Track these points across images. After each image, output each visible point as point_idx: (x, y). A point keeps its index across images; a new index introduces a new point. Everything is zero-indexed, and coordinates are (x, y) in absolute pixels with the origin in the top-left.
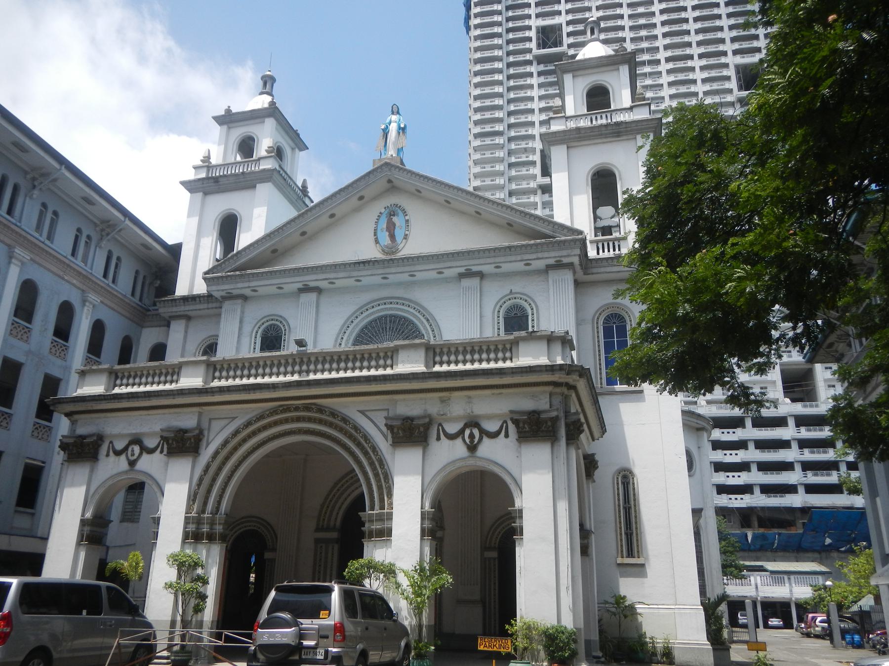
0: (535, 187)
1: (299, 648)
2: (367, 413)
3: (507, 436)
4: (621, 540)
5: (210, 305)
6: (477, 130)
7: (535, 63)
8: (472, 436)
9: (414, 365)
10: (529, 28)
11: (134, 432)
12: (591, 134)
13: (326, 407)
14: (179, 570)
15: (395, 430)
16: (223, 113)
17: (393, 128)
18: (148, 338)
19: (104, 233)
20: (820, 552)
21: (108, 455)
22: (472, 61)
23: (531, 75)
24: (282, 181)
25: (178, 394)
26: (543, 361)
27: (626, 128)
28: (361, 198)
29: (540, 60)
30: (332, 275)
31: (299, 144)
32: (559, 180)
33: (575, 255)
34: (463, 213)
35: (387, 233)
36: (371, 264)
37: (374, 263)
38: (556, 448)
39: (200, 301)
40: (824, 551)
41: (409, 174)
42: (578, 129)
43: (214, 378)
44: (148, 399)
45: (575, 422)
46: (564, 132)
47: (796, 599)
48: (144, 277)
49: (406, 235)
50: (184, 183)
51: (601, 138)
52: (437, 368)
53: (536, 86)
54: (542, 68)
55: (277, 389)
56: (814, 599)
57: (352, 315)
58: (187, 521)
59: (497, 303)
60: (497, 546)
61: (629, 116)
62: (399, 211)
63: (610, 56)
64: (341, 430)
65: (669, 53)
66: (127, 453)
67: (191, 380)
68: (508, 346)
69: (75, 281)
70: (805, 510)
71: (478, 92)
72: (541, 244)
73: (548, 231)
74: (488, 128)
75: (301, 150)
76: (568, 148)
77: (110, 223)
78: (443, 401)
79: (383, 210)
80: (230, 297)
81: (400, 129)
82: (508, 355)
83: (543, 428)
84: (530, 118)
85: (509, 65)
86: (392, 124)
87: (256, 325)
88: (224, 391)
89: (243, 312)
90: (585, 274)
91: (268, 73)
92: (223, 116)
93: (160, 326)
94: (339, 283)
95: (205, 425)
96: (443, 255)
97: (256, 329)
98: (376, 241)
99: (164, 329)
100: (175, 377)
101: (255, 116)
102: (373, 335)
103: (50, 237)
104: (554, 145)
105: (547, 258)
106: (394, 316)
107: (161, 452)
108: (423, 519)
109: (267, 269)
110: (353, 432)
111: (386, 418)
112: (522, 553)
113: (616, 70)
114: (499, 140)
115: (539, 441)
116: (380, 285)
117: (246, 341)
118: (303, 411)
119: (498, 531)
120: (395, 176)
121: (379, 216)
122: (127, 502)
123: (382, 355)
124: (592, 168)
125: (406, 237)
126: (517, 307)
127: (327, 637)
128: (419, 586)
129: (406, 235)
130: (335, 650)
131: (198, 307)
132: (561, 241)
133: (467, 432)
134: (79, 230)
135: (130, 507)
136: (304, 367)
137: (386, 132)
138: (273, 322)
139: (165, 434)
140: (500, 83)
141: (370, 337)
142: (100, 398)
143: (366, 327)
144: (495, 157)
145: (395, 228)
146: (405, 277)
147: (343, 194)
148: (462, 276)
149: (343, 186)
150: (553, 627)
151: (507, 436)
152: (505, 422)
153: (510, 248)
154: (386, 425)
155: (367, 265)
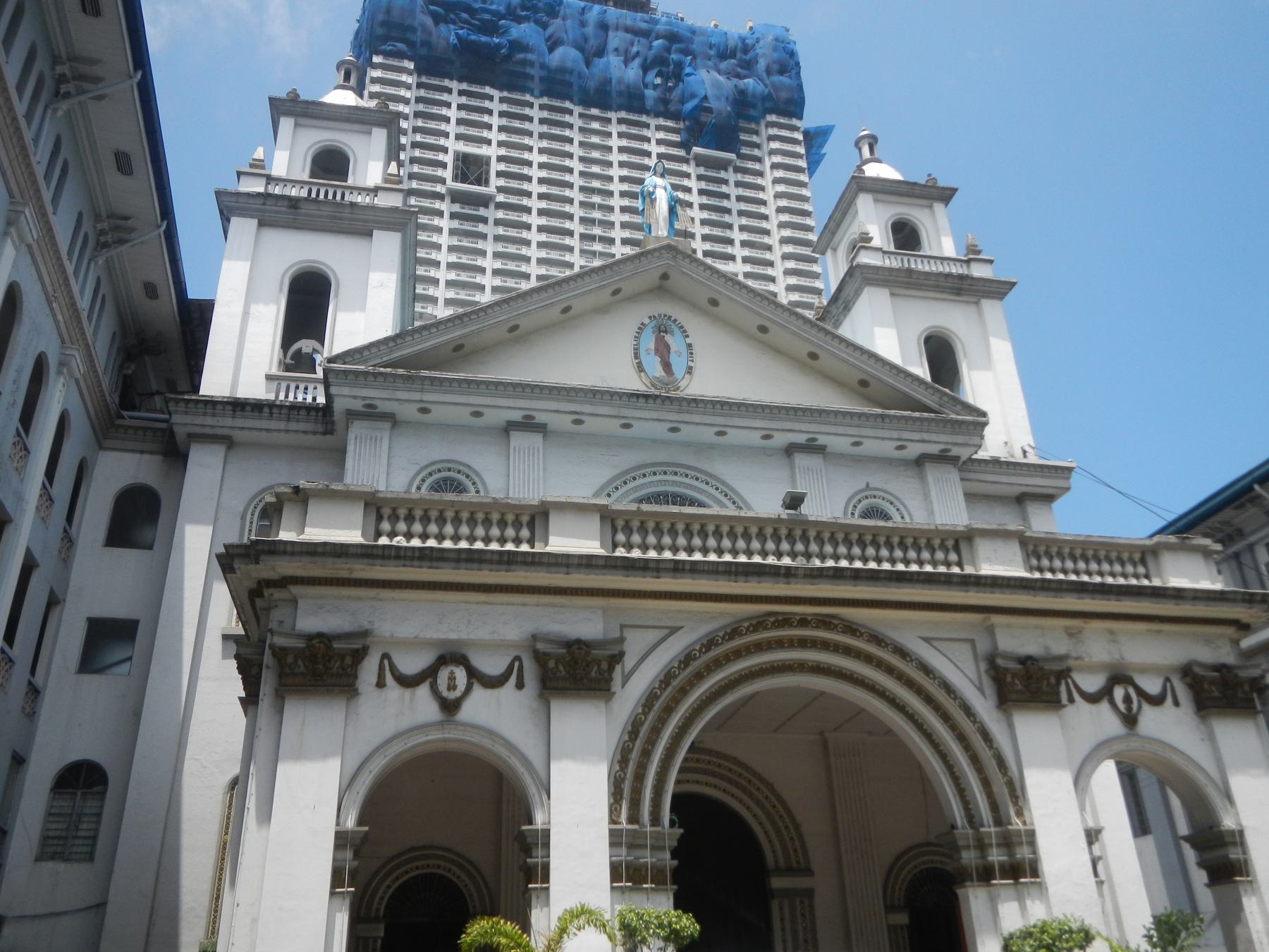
7: (448, 199)
8: (1127, 699)
9: (1009, 568)
10: (445, 150)
11: (453, 636)
12: (926, 282)
13: (860, 625)
21: (381, 684)
23: (440, 214)
25: (579, 566)
27: (971, 285)
29: (456, 197)
30: (587, 408)
34: (777, 351)
36: (658, 401)
37: (663, 401)
39: (271, 413)
44: (504, 567)
49: (691, 368)
51: (938, 291)
54: (457, 208)
55: (792, 580)
58: (615, 839)
59: (850, 500)
62: (673, 326)
78: (1072, 634)
79: (647, 321)
80: (370, 414)
88: (683, 570)
93: (142, 452)
94: (591, 424)
96: (780, 409)
104: (871, 285)
106: (681, 497)
113: (927, 206)
116: (655, 442)
118: (817, 627)
120: (685, 270)
121: (640, 328)
125: (690, 370)
129: (691, 368)
131: (264, 424)
133: (1119, 693)
135: (60, 826)
138: (451, 474)
142: (387, 553)
146: (708, 434)
155: (651, 401)
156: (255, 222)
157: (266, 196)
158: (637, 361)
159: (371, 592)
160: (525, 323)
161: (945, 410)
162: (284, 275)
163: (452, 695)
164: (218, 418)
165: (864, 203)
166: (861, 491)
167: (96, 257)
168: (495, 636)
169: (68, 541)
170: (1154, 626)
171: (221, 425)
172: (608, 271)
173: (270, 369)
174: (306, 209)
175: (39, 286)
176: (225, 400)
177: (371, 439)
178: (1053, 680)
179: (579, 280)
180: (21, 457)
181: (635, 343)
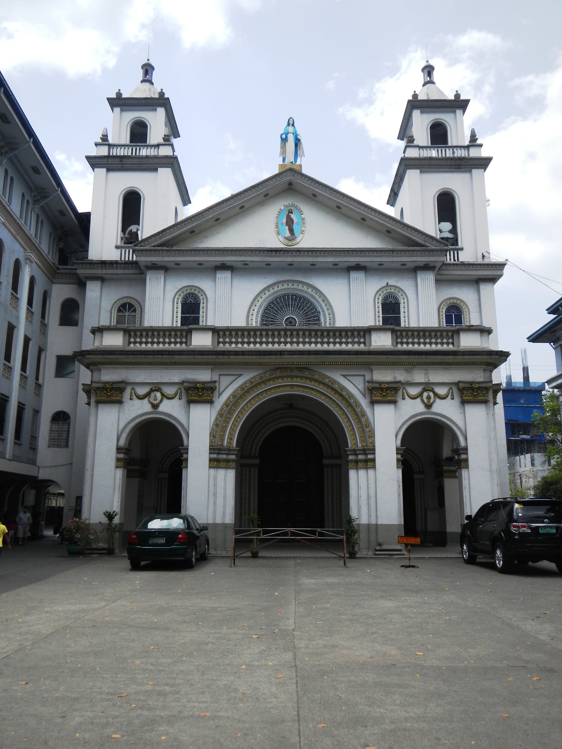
5: (127, 271)
8: (429, 398)
16: (115, 96)
27: (466, 163)
30: (248, 259)
35: (287, 228)
48: (54, 239)
73: (420, 241)
76: (420, 172)
77: (45, 191)
79: (283, 208)
80: (155, 267)
81: (296, 139)
86: (289, 134)
93: (69, 284)
98: (278, 233)
102: (278, 309)
104: (410, 169)
106: (295, 296)
121: (279, 212)
122: (51, 431)
125: (302, 232)
126: (392, 296)
131: (114, 271)
133: (425, 395)
141: (276, 311)
145: (293, 223)
153: (393, 251)
156: (105, 169)
157: (108, 157)
158: (277, 229)
162: (120, 196)
163: (155, 402)
164: (96, 270)
165: (416, 114)
167: (34, 208)
169: (44, 326)
171: (97, 273)
173: (117, 243)
175: (10, 234)
176: (98, 262)
177: (156, 279)
179: (246, 193)
180: (16, 302)
181: (276, 220)
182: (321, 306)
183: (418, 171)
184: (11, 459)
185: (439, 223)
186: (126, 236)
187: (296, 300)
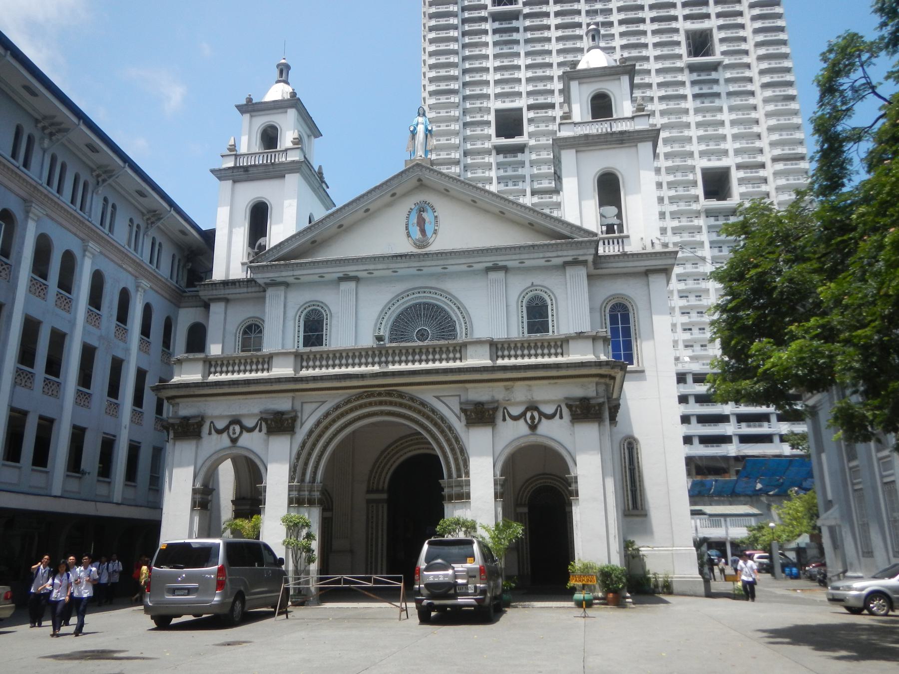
0: (490, 147)
1: (455, 585)
2: (441, 398)
3: (561, 417)
4: (627, 495)
5: (250, 290)
6: (432, 87)
7: (490, 20)
8: (532, 418)
11: (234, 413)
14: (289, 528)
15: (469, 413)
17: (421, 129)
18: (186, 318)
19: (149, 222)
20: (752, 497)
21: (210, 433)
22: (427, 16)
23: (485, 32)
24: (309, 172)
25: (276, 382)
26: (590, 357)
28: (393, 195)
30: (371, 267)
31: (315, 132)
32: (570, 184)
33: (590, 254)
34: (486, 211)
35: (418, 228)
36: (408, 257)
38: (601, 427)
40: (754, 495)
41: (439, 175)
42: (587, 136)
43: (302, 367)
45: (616, 406)
46: (574, 138)
47: (732, 539)
49: (436, 230)
50: (213, 171)
52: (500, 362)
53: (491, 44)
54: (497, 25)
56: (749, 538)
57: (389, 303)
58: (290, 489)
60: (527, 502)
61: (631, 126)
62: (428, 208)
63: (613, 67)
64: (420, 412)
65: (622, 16)
66: (228, 433)
67: (282, 370)
68: (559, 343)
69: (130, 269)
70: (738, 459)
71: (433, 48)
72: (561, 244)
74: (443, 86)
75: (316, 137)
79: (413, 207)
80: (274, 284)
82: (559, 351)
83: (592, 412)
84: (485, 77)
85: (464, 21)
86: (419, 126)
87: (299, 310)
88: (317, 380)
89: (285, 298)
90: (596, 268)
91: (283, 61)
92: (245, 105)
93: (197, 307)
94: (376, 273)
95: (298, 407)
96: (473, 251)
97: (299, 313)
99: (201, 310)
100: (266, 366)
101: (278, 106)
103: (111, 229)
104: (564, 149)
105: (566, 256)
107: (260, 431)
108: (495, 484)
109: (310, 260)
110: (431, 414)
111: (461, 403)
112: (578, 510)
114: (455, 99)
115: (589, 422)
116: (413, 276)
117: (290, 324)
119: (528, 490)
121: (409, 212)
123: (451, 349)
124: (598, 172)
125: (435, 232)
127: (475, 577)
128: (499, 538)
129: (436, 230)
130: (482, 586)
131: (238, 291)
132: (578, 242)
133: (529, 415)
134: (131, 220)
136: (383, 359)
137: (414, 133)
139: (264, 416)
140: (455, 40)
143: (402, 313)
144: (450, 116)
146: (439, 269)
147: (377, 191)
148: (488, 270)
149: (378, 184)
150: (607, 567)
151: (561, 417)
152: (559, 406)
153: (533, 246)
154: (461, 409)
155: (403, 258)
159: (204, 399)
160: (345, 223)
161: (575, 236)
166: (529, 287)
168: (250, 412)
170: (552, 381)
172: (384, 186)
174: (252, 170)
178: (491, 412)
182: (455, 315)
183: (574, 151)
184: (120, 502)
185: (600, 208)
186: (256, 250)
187: (428, 309)
